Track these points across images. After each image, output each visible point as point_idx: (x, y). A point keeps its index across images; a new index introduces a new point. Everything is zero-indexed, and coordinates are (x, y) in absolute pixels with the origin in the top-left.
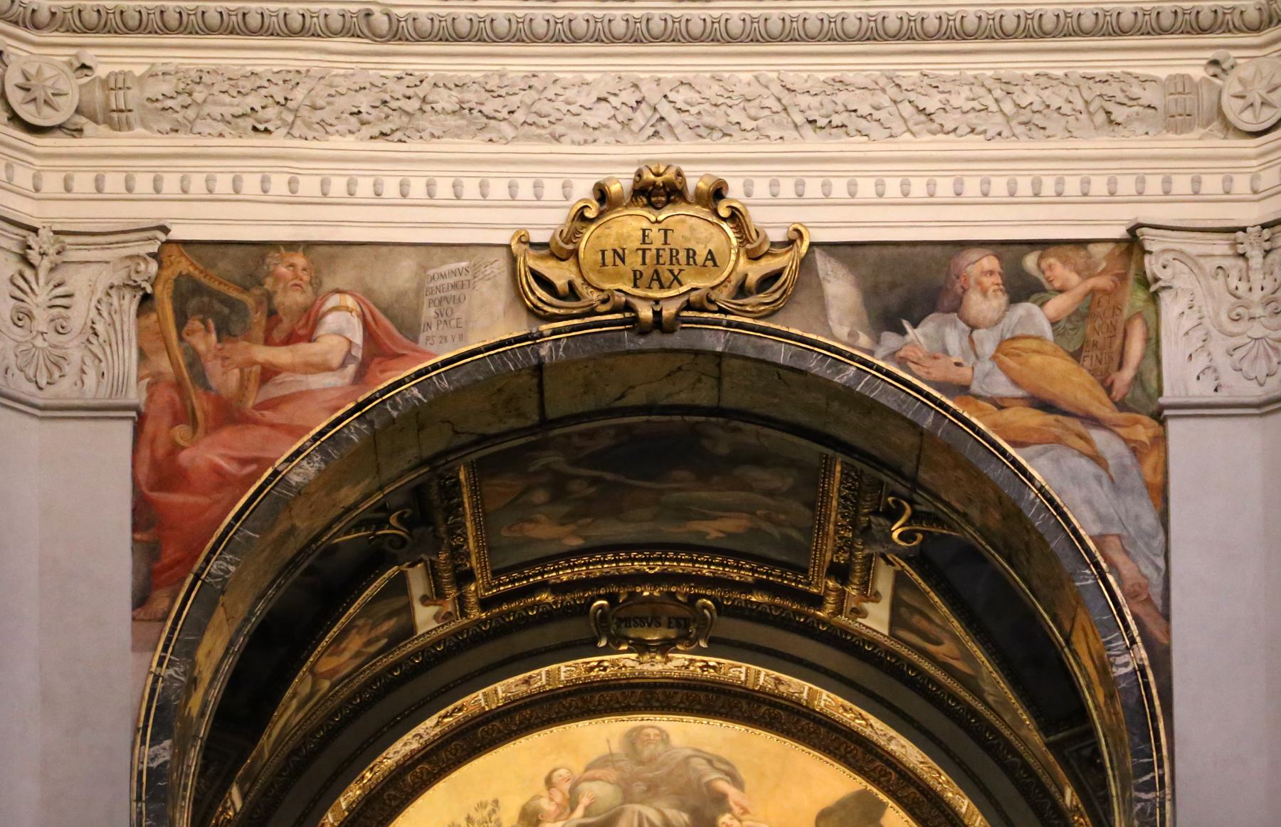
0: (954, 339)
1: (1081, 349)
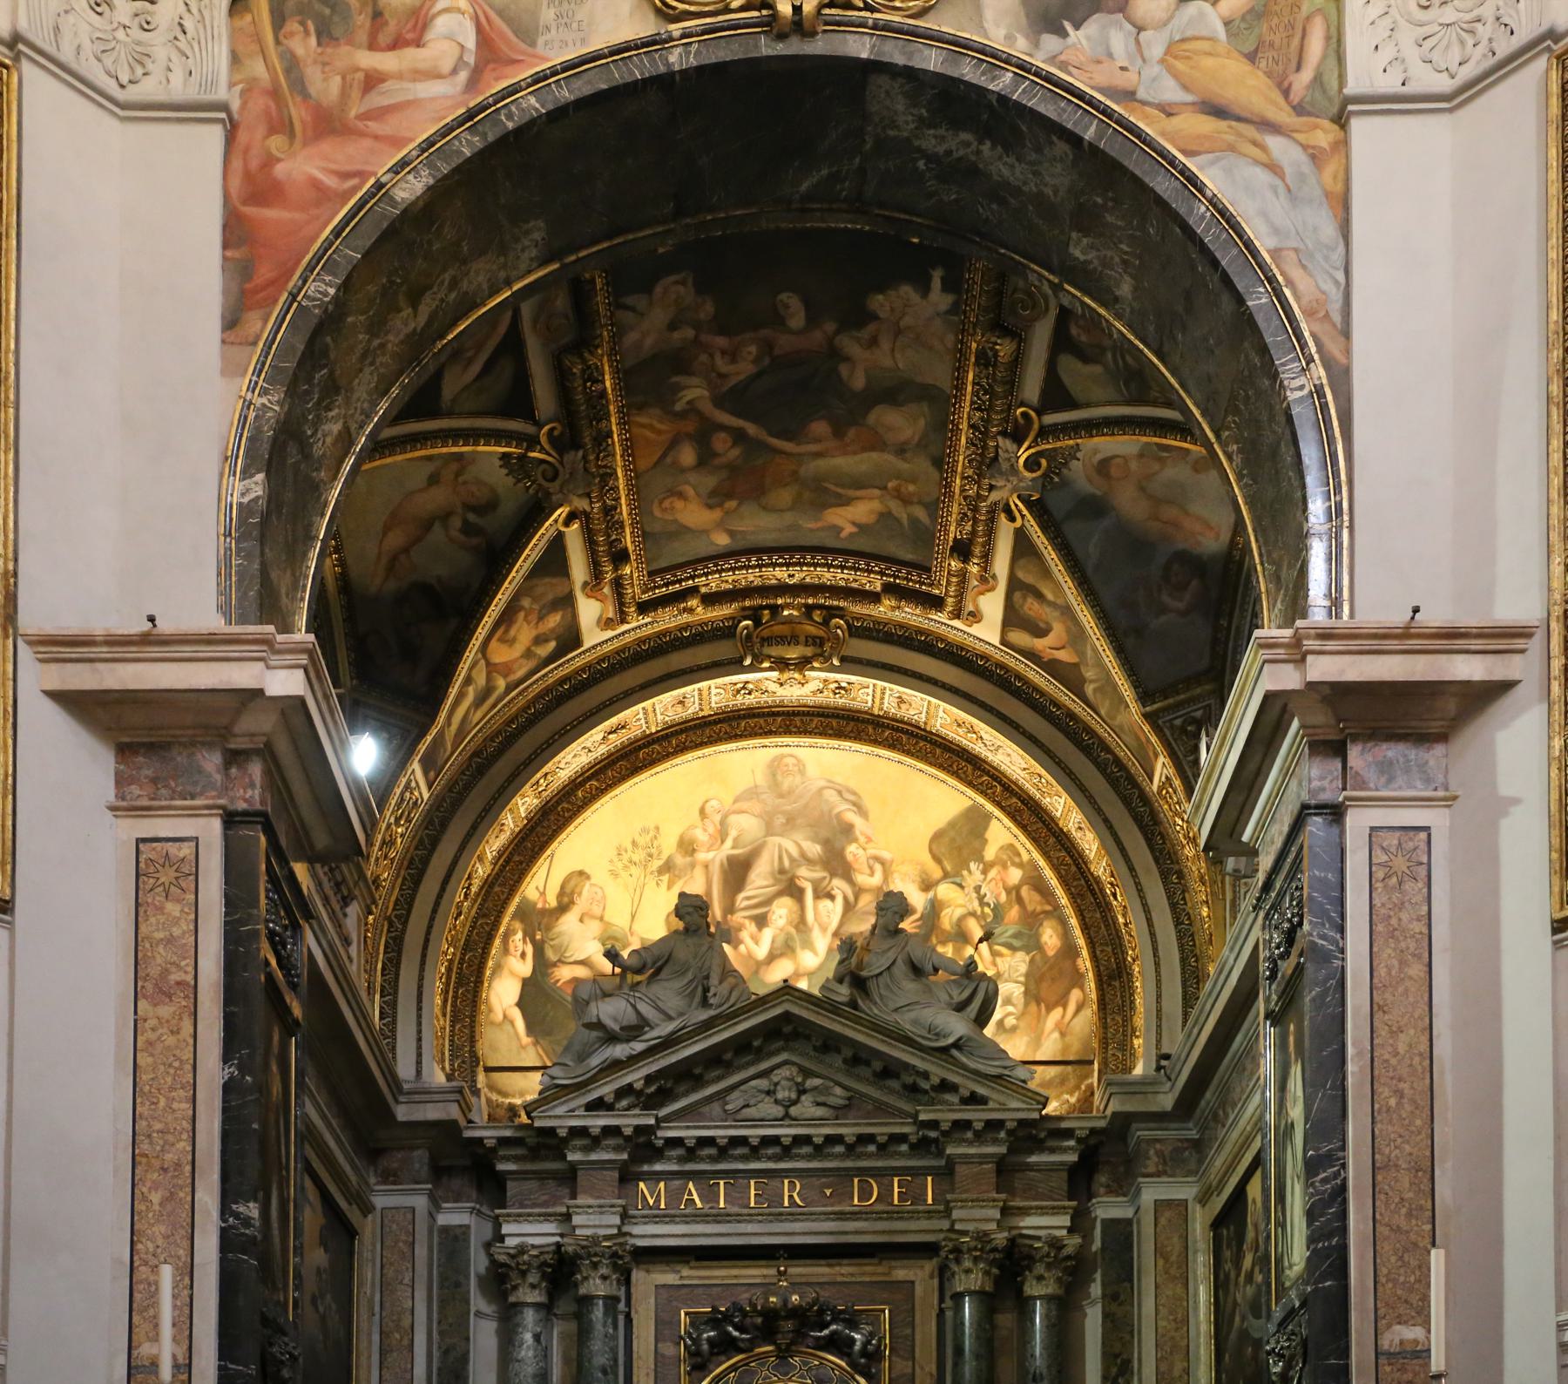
0: (1119, 40)
1: (1256, 51)
